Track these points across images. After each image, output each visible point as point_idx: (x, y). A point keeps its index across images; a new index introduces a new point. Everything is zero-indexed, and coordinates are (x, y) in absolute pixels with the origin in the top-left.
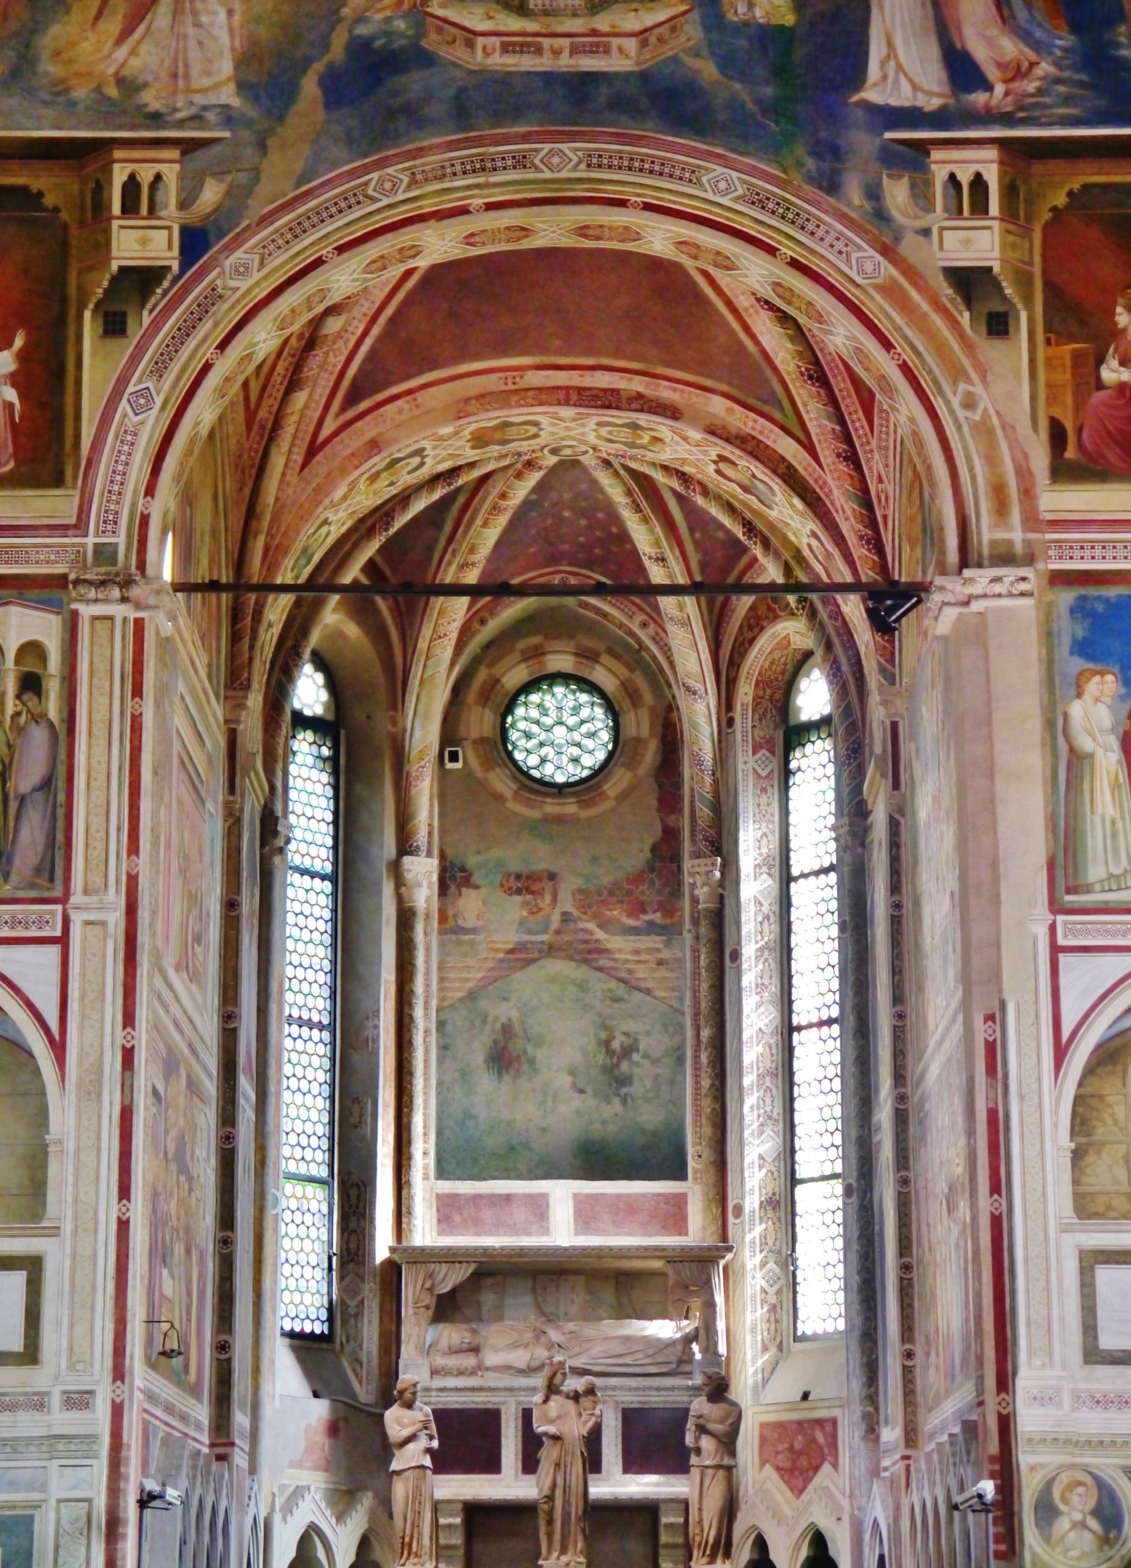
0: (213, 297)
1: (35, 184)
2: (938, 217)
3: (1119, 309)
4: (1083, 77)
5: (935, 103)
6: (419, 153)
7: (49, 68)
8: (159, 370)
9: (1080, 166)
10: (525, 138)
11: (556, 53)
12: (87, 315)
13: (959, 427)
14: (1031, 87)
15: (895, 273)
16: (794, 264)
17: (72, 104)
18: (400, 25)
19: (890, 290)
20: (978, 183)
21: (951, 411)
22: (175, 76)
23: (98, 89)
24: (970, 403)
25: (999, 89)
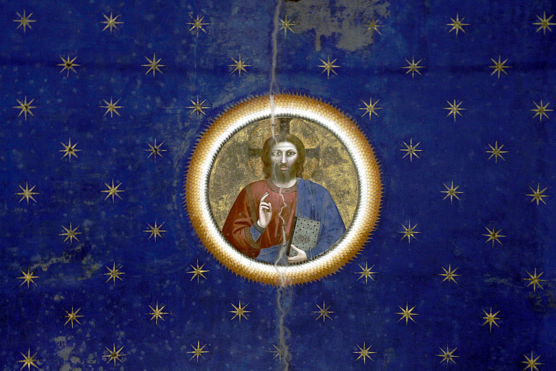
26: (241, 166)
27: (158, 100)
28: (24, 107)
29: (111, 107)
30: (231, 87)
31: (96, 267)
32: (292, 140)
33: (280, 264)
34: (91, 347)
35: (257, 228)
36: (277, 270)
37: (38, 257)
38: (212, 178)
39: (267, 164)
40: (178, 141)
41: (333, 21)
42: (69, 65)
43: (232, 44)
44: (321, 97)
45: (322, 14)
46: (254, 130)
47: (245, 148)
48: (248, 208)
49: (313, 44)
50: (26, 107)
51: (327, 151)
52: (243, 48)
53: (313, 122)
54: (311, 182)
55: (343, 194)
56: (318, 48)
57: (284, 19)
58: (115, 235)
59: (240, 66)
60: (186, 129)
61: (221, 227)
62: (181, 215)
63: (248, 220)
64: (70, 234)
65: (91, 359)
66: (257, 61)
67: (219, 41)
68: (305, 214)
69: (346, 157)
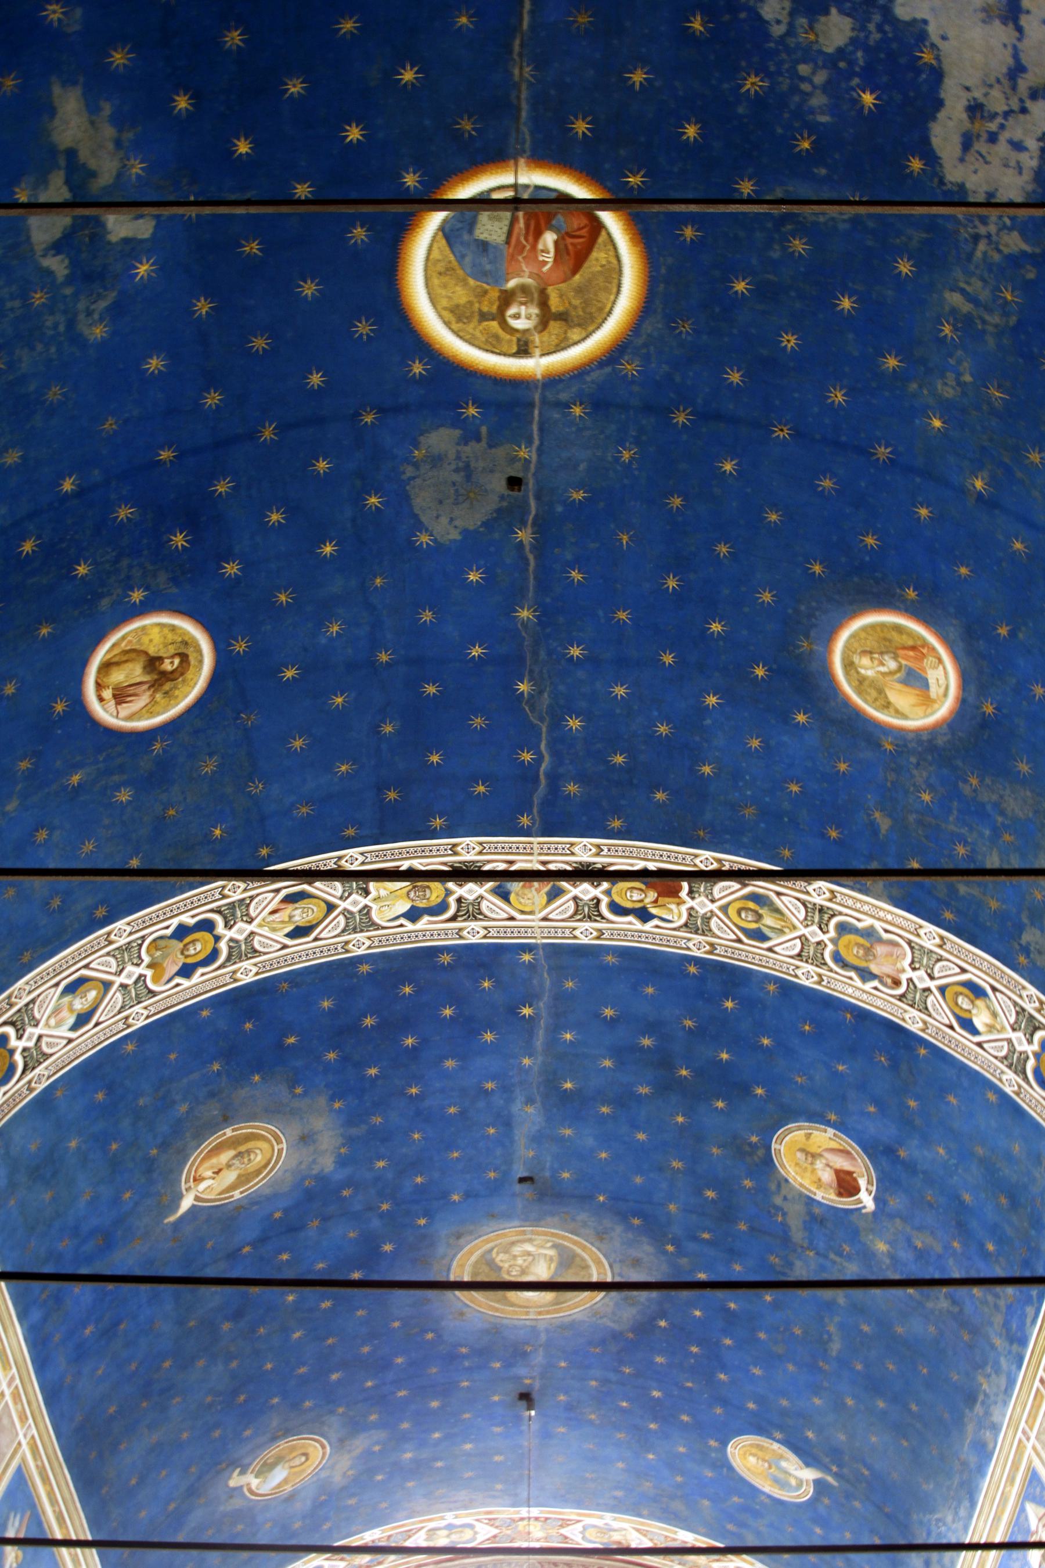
26: (576, 302)
27: (678, 379)
28: (839, 397)
29: (735, 377)
30: (589, 388)
32: (513, 331)
35: (556, 230)
36: (530, 179)
37: (842, 227)
38: (615, 290)
40: (655, 334)
41: (467, 457)
42: (782, 430)
43: (587, 433)
44: (478, 378)
45: (481, 464)
46: (561, 341)
47: (572, 321)
48: (568, 253)
49: (490, 434)
50: (836, 396)
51: (469, 319)
52: (574, 429)
53: (487, 351)
54: (488, 284)
55: (448, 271)
56: (484, 430)
57: (525, 459)
58: (742, 234)
59: (577, 411)
60: (645, 345)
61: (603, 233)
62: (655, 250)
63: (569, 241)
65: (785, 84)
66: (557, 416)
67: (602, 436)
68: (496, 247)
69: (445, 314)
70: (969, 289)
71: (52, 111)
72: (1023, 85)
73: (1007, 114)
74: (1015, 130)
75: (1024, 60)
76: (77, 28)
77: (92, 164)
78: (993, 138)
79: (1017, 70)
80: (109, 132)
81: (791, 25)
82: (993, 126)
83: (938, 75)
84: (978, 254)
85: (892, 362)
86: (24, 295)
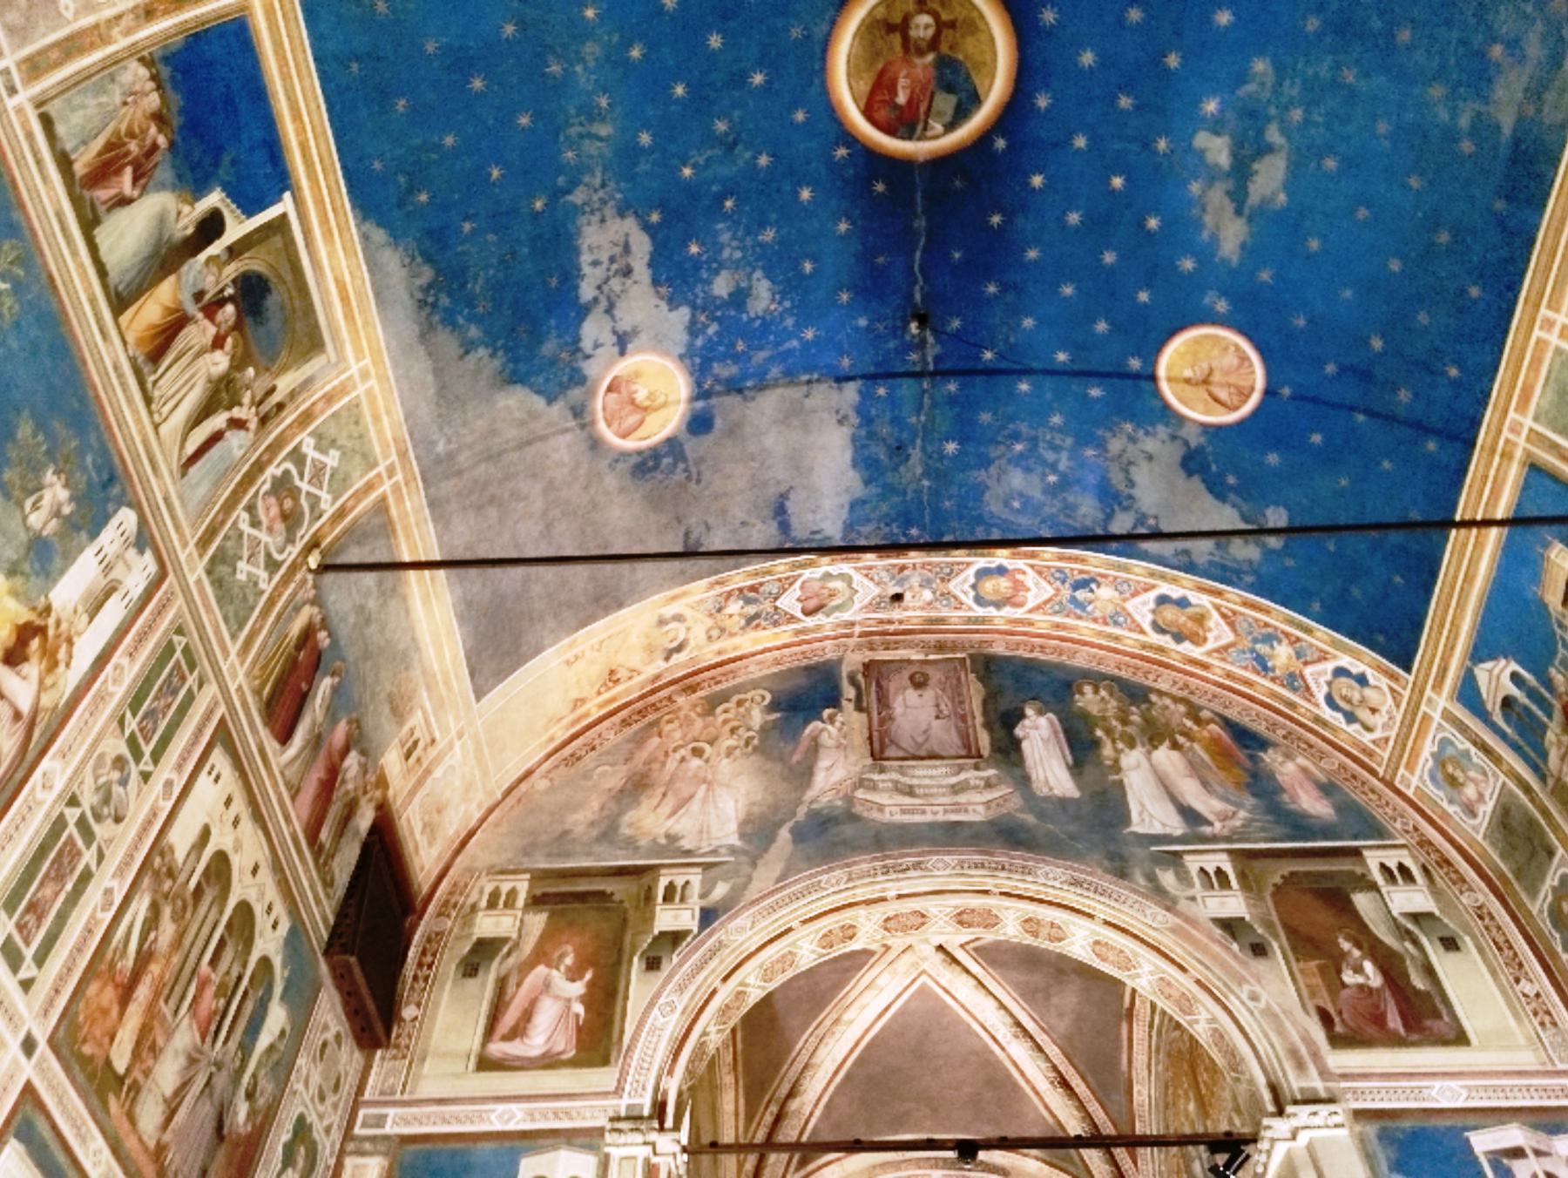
0: (720, 945)
1: (609, 890)
2: (1198, 889)
3: (1341, 940)
4: (1269, 818)
5: (1178, 832)
6: (855, 863)
7: (626, 831)
8: (681, 989)
9: (1284, 862)
10: (919, 855)
11: (935, 813)
12: (636, 959)
13: (1252, 1013)
14: (1238, 823)
15: (1178, 921)
16: (1107, 923)
17: (637, 848)
18: (839, 803)
19: (1175, 930)
20: (1219, 872)
21: (1243, 1003)
22: (701, 832)
23: (654, 841)
24: (1254, 997)
25: (1218, 825)
31: (748, 155)
32: (928, 12)
33: (919, 139)
34: (748, 232)
39: (906, 39)
64: (721, 127)
70: (599, 144)
71: (1243, 246)
72: (604, 304)
73: (608, 279)
74: (599, 272)
75: (608, 318)
76: (1211, 293)
77: (1227, 201)
78: (612, 260)
79: (609, 310)
80: (1208, 219)
81: (750, 279)
82: (615, 267)
83: (656, 282)
84: (598, 174)
85: (636, 53)
86: (1307, 122)
